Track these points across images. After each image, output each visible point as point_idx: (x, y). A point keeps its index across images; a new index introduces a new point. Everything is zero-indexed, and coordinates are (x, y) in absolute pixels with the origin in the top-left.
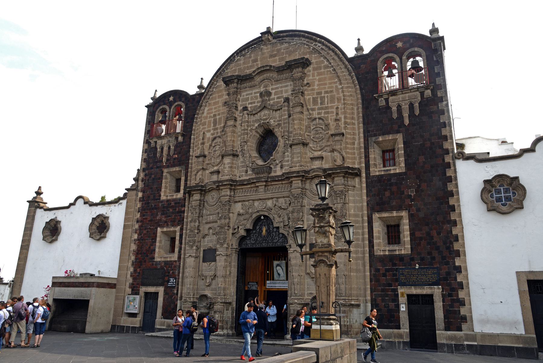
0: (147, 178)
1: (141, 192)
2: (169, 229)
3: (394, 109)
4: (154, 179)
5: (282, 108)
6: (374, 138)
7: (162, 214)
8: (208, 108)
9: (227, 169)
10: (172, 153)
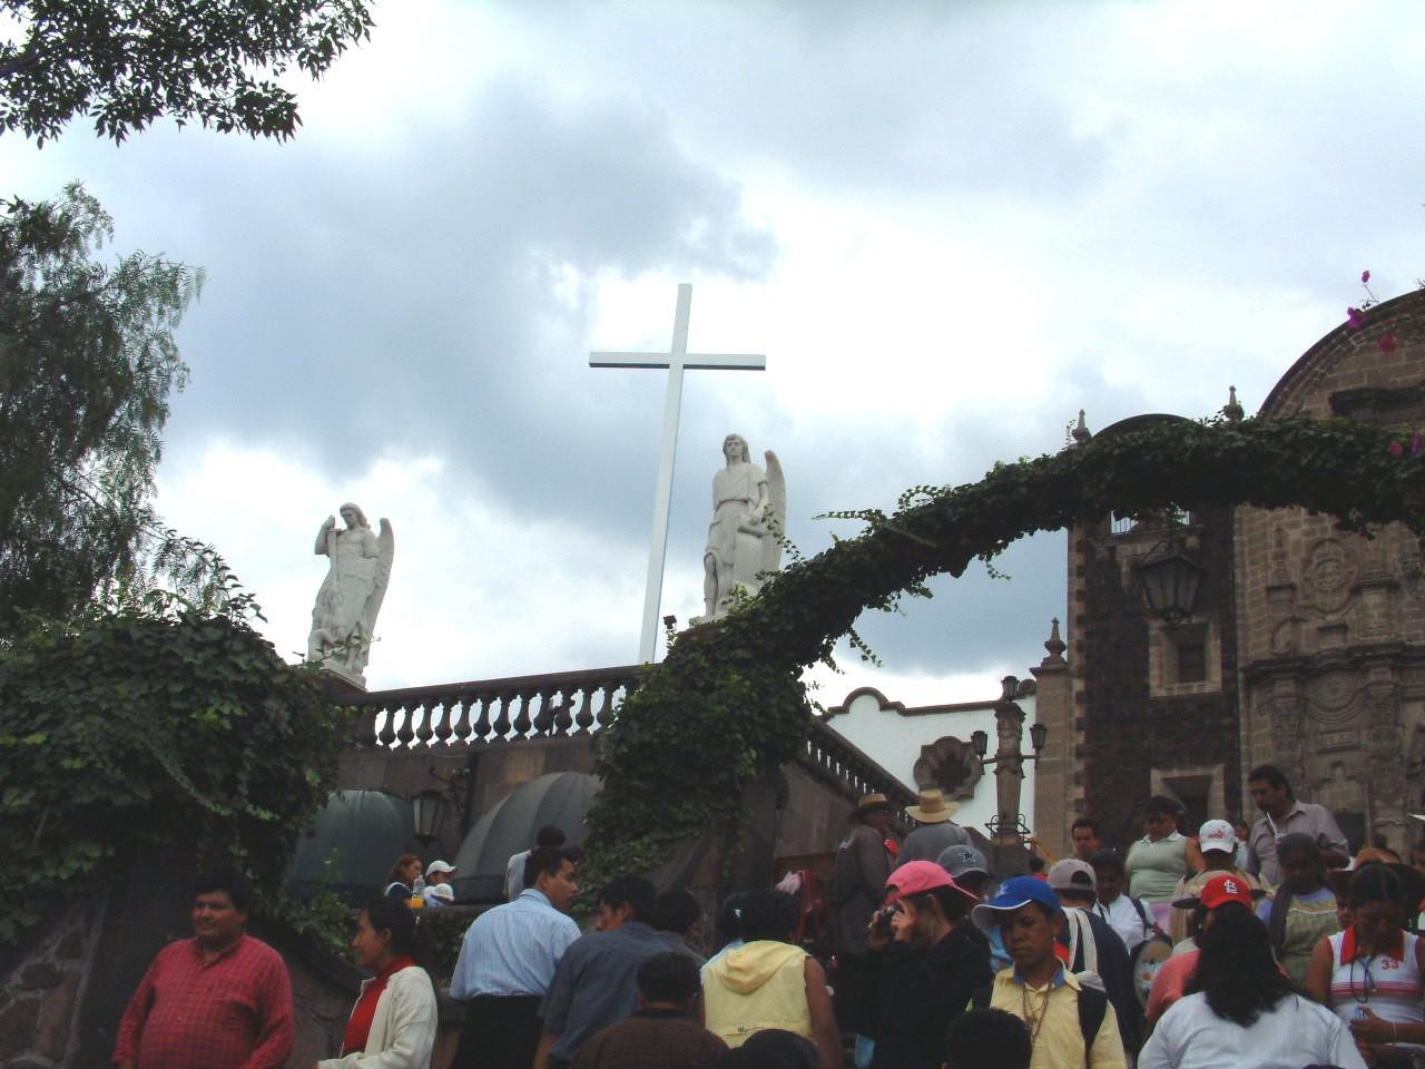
1: (1080, 677)
2: (1187, 773)
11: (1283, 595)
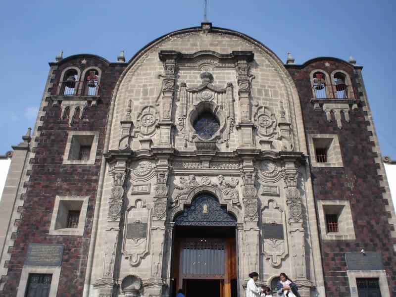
0: (44, 138)
1: (34, 152)
2: (72, 199)
3: (328, 114)
4: (53, 141)
5: (225, 92)
6: (313, 135)
7: (62, 181)
8: (136, 78)
9: (165, 139)
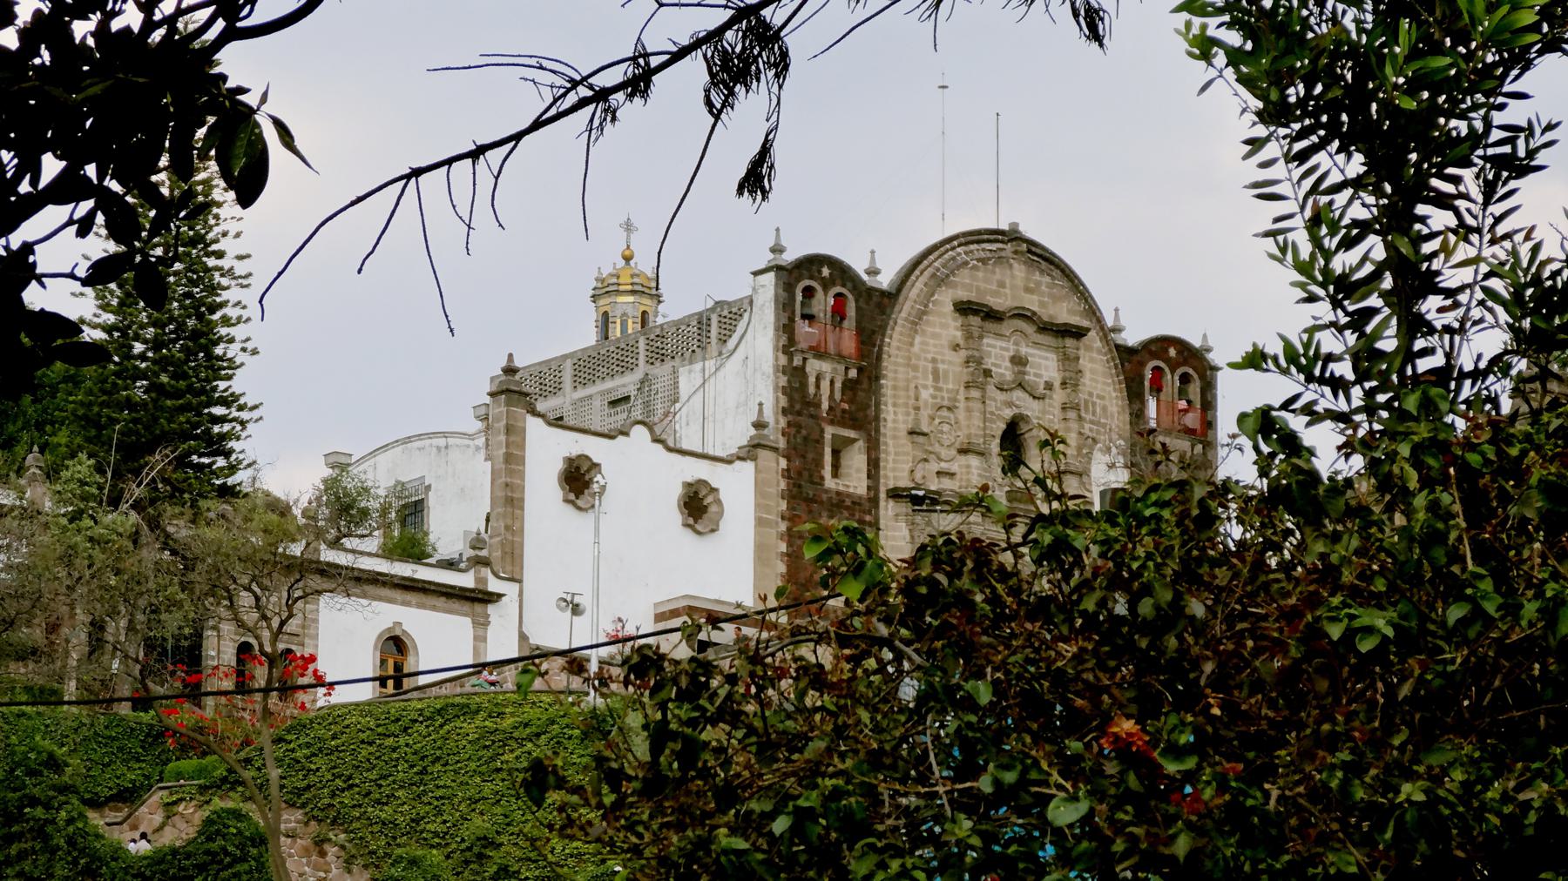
10: (838, 396)
11: (921, 439)
